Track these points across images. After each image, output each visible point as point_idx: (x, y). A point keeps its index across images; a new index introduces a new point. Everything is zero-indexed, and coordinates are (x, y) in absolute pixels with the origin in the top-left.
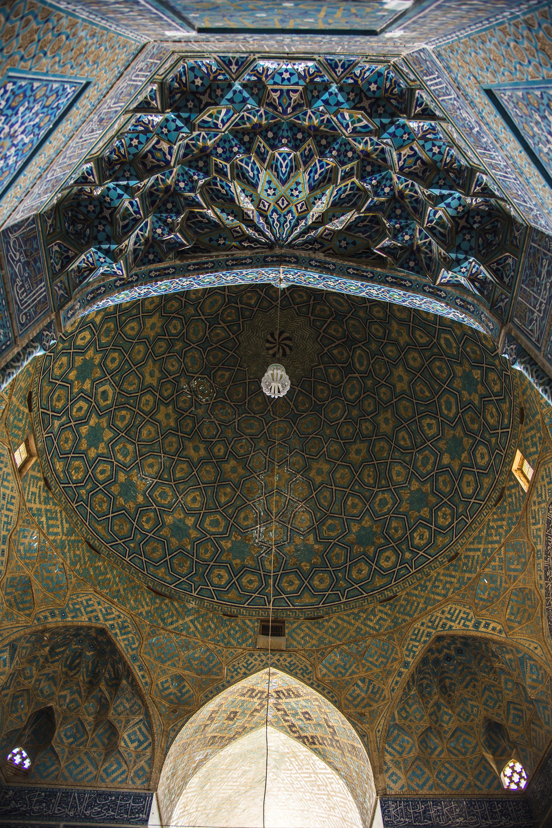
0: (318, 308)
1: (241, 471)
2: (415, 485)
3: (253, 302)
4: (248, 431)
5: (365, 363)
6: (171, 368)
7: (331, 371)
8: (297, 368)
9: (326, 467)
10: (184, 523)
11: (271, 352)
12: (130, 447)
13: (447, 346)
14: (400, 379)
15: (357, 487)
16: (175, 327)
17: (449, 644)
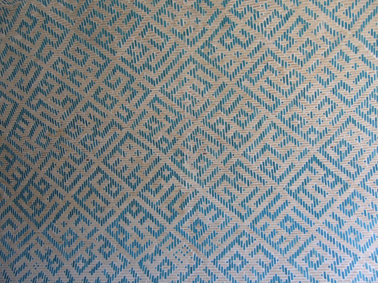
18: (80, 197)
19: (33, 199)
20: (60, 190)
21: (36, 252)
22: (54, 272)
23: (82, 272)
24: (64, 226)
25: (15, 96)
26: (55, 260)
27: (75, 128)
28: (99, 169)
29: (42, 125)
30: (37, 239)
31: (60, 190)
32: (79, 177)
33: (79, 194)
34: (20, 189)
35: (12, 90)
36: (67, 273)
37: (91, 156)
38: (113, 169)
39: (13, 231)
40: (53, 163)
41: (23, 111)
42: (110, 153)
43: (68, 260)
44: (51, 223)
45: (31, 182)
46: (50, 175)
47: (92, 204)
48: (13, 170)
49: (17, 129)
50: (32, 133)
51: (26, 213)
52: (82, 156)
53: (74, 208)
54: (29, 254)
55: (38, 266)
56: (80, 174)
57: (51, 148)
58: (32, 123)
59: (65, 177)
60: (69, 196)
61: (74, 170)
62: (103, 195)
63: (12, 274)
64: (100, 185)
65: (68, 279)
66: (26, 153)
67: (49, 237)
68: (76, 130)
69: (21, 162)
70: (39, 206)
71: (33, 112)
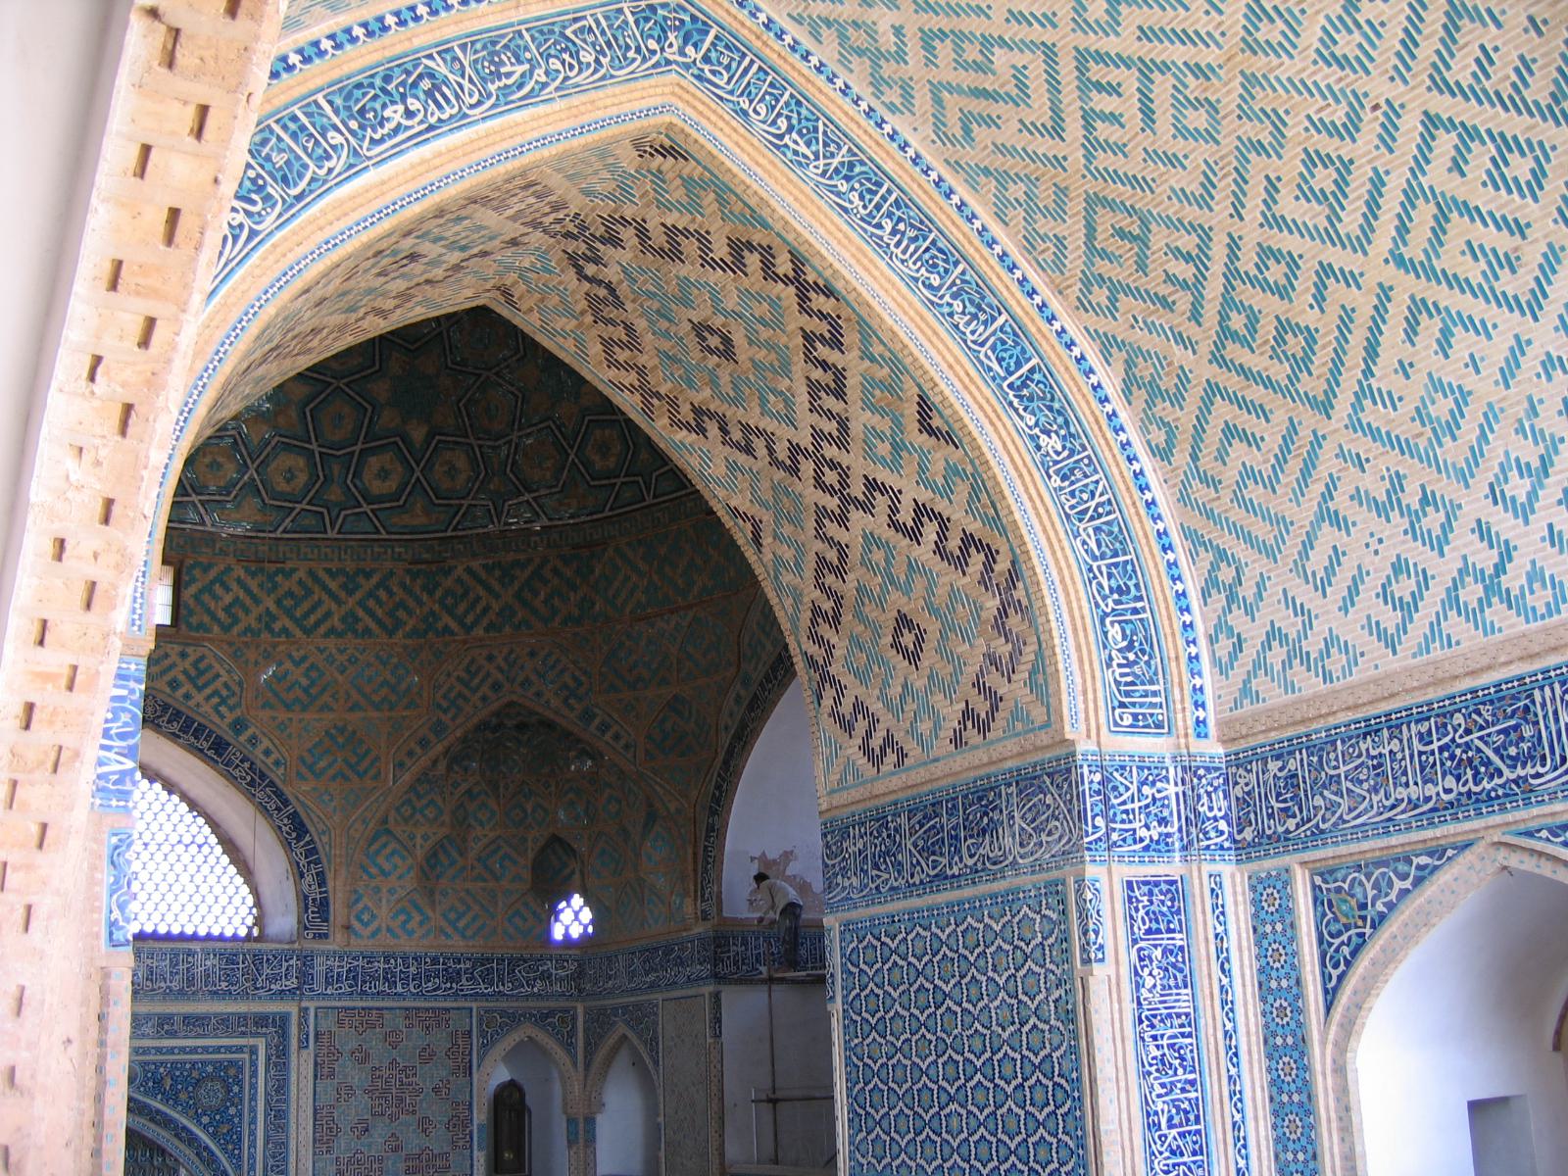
18: (1414, 251)
19: (1267, 329)
20: (1340, 258)
21: (1356, 496)
22: (1439, 545)
23: (1533, 512)
24: (1408, 377)
25: (1030, 24)
26: (1424, 501)
27: (1272, 21)
28: (1431, 121)
29: (1164, 68)
30: (1341, 454)
31: (1340, 258)
32: (1377, 183)
33: (1405, 244)
34: (1210, 313)
35: (1010, 11)
36: (1482, 531)
37: (1378, 87)
38: (1479, 96)
39: (1256, 459)
40: (1267, 177)
41: (1082, 58)
42: (1442, 40)
43: (1467, 486)
44: (1360, 382)
45: (1231, 274)
46: (1280, 223)
47: (1469, 257)
48: (1162, 263)
49: (1098, 124)
50: (1148, 113)
51: (1268, 383)
52: (1350, 104)
53: (1412, 298)
54: (1336, 512)
55: (1380, 541)
56: (1375, 170)
57: (1233, 131)
58: (1130, 80)
59: (1331, 206)
60: (1375, 266)
61: (1347, 165)
62: (1492, 207)
63: (1312, 594)
64: (1463, 174)
65: (1495, 552)
66: (1166, 186)
67: (1374, 434)
68: (1280, 25)
69: (1168, 223)
70: (1295, 344)
71: (1110, 45)
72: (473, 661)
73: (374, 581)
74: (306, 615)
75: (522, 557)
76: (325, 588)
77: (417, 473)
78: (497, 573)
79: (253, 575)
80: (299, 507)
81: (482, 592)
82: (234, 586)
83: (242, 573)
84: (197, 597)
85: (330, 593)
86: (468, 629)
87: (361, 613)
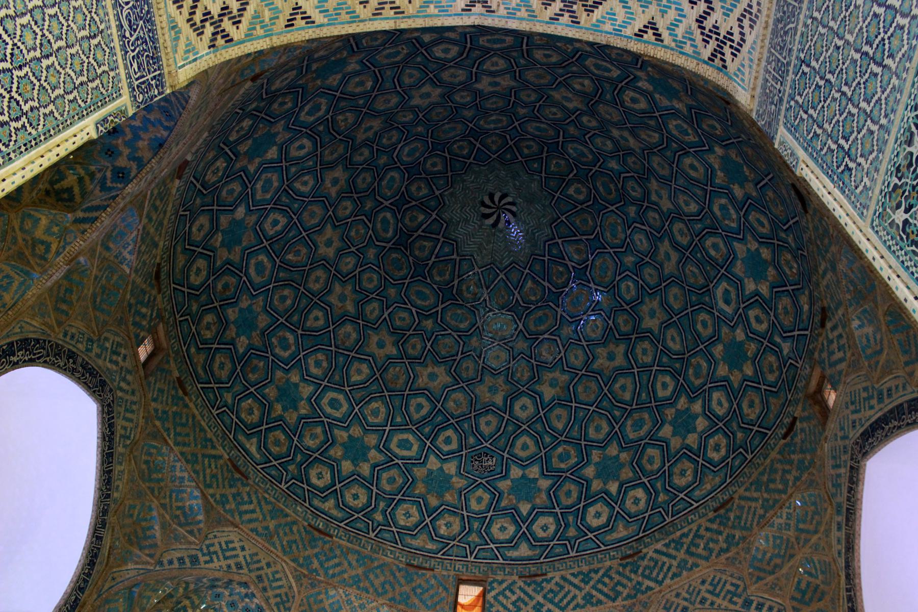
0: (447, 277)
1: (556, 95)
2: (272, 153)
3: (529, 284)
4: (542, 126)
5: (379, 225)
6: (644, 241)
7: (424, 191)
8: (473, 182)
9: (416, 101)
10: (655, 88)
11: (509, 199)
12: (716, 209)
13: (285, 339)
14: (329, 243)
15: (361, 102)
16: (628, 289)
17: (136, 137)
72: (668, 601)
73: (600, 573)
74: (561, 600)
75: (686, 530)
76: (571, 583)
77: (617, 509)
78: (673, 545)
79: (529, 585)
80: (552, 543)
81: (665, 559)
82: (518, 591)
83: (522, 584)
84: (495, 598)
85: (575, 586)
86: (660, 583)
87: (594, 593)
